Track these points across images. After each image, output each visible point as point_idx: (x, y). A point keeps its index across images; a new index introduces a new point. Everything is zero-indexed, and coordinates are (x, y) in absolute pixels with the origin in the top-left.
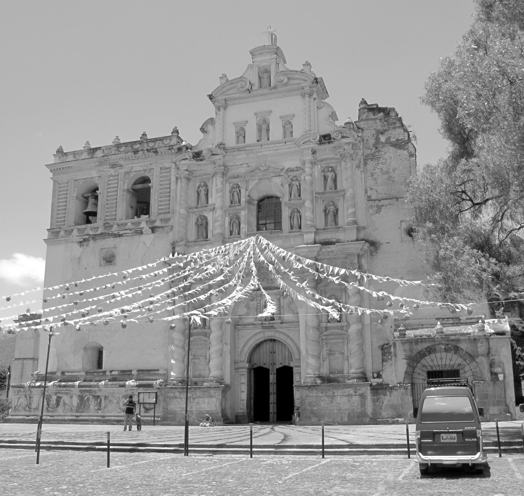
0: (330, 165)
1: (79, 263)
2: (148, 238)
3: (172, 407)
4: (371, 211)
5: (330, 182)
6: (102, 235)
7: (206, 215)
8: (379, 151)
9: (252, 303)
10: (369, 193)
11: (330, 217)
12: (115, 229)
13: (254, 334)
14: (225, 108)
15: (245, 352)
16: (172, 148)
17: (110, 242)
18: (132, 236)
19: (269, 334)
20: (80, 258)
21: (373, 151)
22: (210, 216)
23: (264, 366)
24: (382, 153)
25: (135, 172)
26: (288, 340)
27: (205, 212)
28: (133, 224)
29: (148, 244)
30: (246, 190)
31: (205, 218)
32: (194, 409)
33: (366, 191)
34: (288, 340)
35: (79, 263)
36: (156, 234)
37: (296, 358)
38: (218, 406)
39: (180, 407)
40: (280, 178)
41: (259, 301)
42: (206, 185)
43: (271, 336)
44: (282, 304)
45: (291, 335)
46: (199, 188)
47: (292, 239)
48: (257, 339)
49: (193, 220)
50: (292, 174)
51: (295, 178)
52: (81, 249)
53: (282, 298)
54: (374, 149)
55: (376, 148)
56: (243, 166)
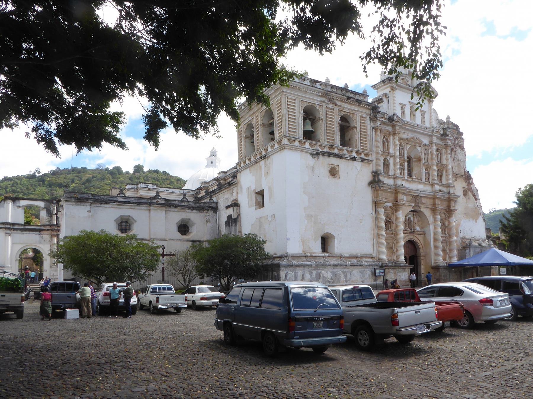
1: (313, 170)
2: (358, 165)
5: (439, 157)
6: (329, 155)
11: (439, 178)
12: (336, 151)
17: (334, 161)
18: (348, 160)
20: (313, 167)
22: (391, 161)
26: (419, 242)
28: (347, 151)
35: (313, 170)
42: (387, 139)
50: (426, 148)
52: (314, 160)
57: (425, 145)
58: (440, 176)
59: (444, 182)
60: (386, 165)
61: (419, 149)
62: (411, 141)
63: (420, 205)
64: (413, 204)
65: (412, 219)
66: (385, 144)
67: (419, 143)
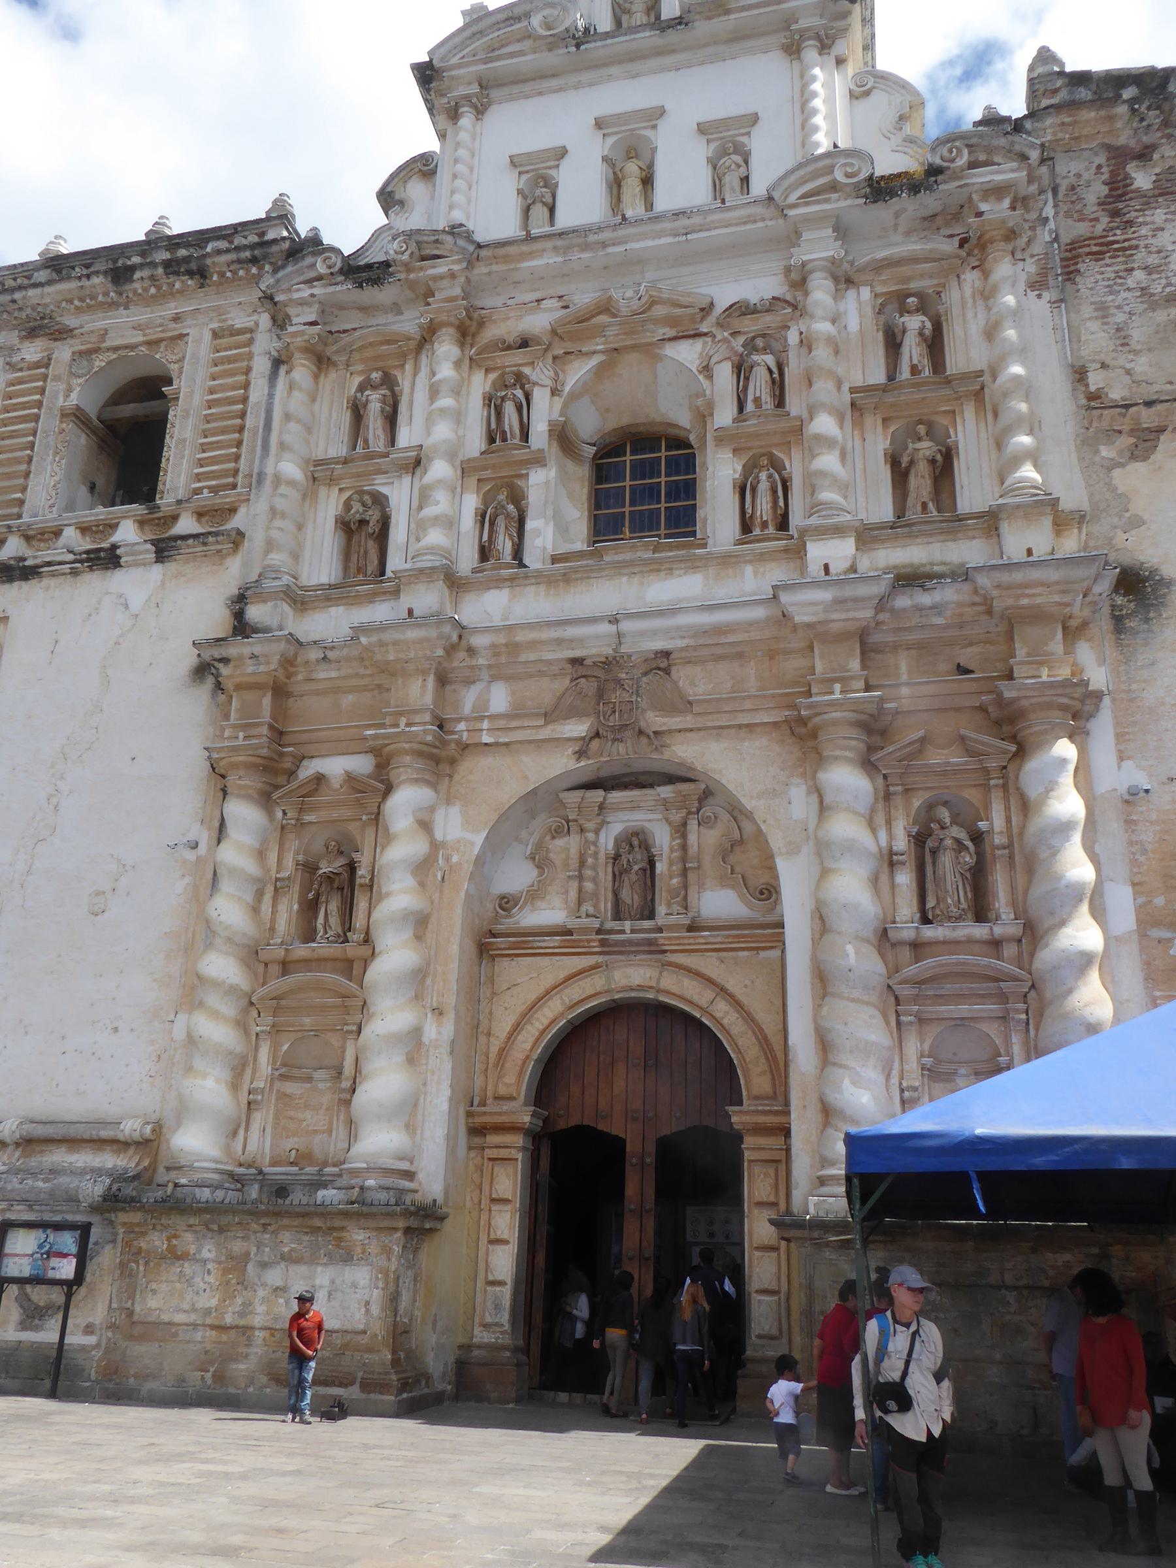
0: (914, 285)
3: (153, 1303)
4: (1106, 452)
7: (384, 490)
8: (1130, 223)
9: (560, 842)
10: (1095, 380)
11: (920, 483)
13: (562, 975)
14: (480, 111)
15: (522, 1056)
16: (265, 257)
18: (74, 573)
19: (633, 977)
21: (1099, 228)
22: (399, 494)
23: (602, 1126)
24: (1144, 231)
25: (116, 349)
26: (721, 1008)
27: (380, 479)
29: (136, 603)
30: (554, 392)
31: (380, 501)
32: (257, 1321)
33: (1080, 374)
34: (721, 1008)
36: (171, 567)
37: (756, 1091)
38: (375, 1310)
39: (194, 1310)
40: (698, 345)
41: (591, 836)
43: (641, 988)
44: (693, 849)
45: (733, 985)
46: (361, 388)
47: (749, 570)
48: (577, 998)
49: (330, 505)
50: (750, 326)
51: (760, 342)
53: (693, 825)
54: (1105, 220)
55: (1115, 214)
56: (546, 304)
57: (742, 309)
58: (925, 478)
59: (973, 491)
60: (365, 534)
61: (687, 353)
62: (600, 331)
63: (654, 720)
64: (578, 728)
65: (662, 839)
66: (377, 407)
67: (671, 321)
